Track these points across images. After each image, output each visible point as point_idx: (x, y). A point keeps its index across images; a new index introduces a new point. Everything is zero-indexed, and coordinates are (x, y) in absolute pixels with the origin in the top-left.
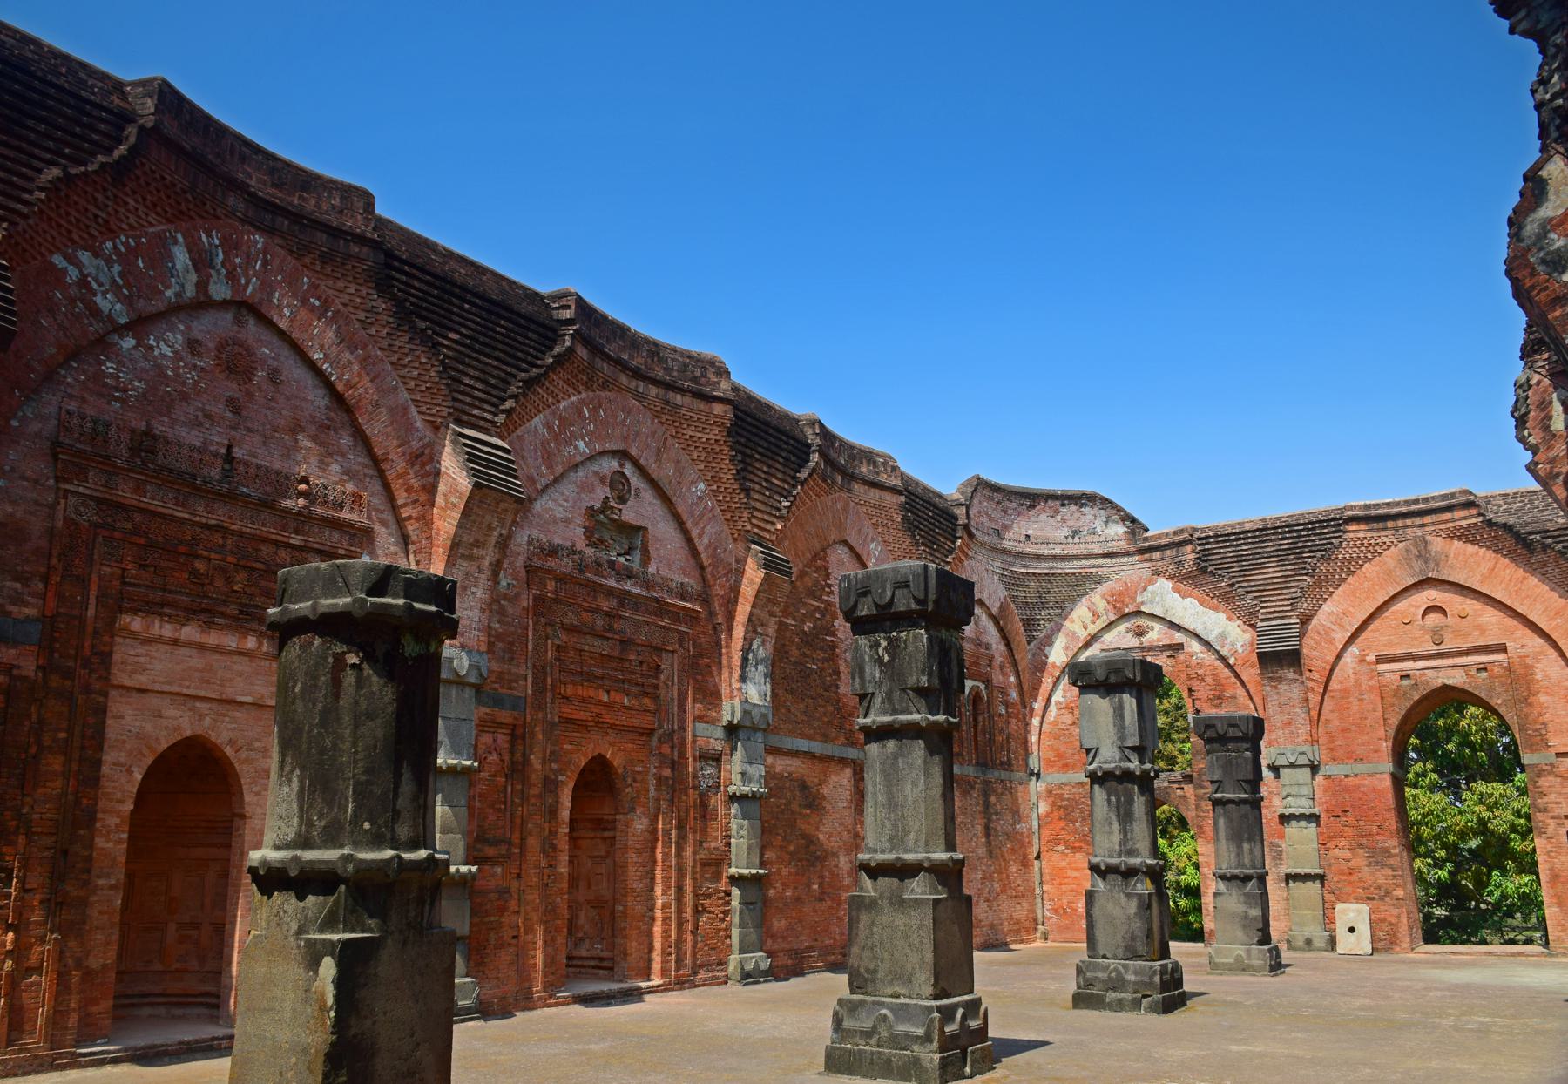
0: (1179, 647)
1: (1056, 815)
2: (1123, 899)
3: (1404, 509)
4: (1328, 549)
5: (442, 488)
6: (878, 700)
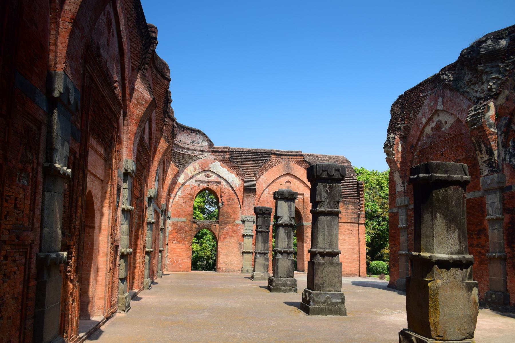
0: (220, 183)
1: (174, 231)
2: (287, 260)
3: (286, 153)
4: (266, 161)
5: (135, 95)
6: (326, 204)
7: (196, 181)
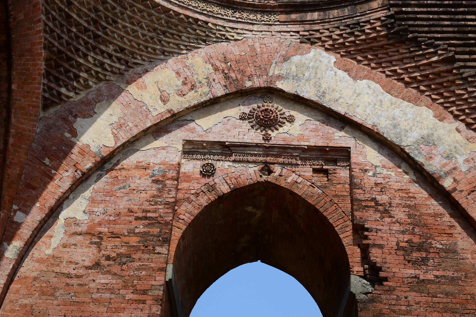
7: (192, 149)
